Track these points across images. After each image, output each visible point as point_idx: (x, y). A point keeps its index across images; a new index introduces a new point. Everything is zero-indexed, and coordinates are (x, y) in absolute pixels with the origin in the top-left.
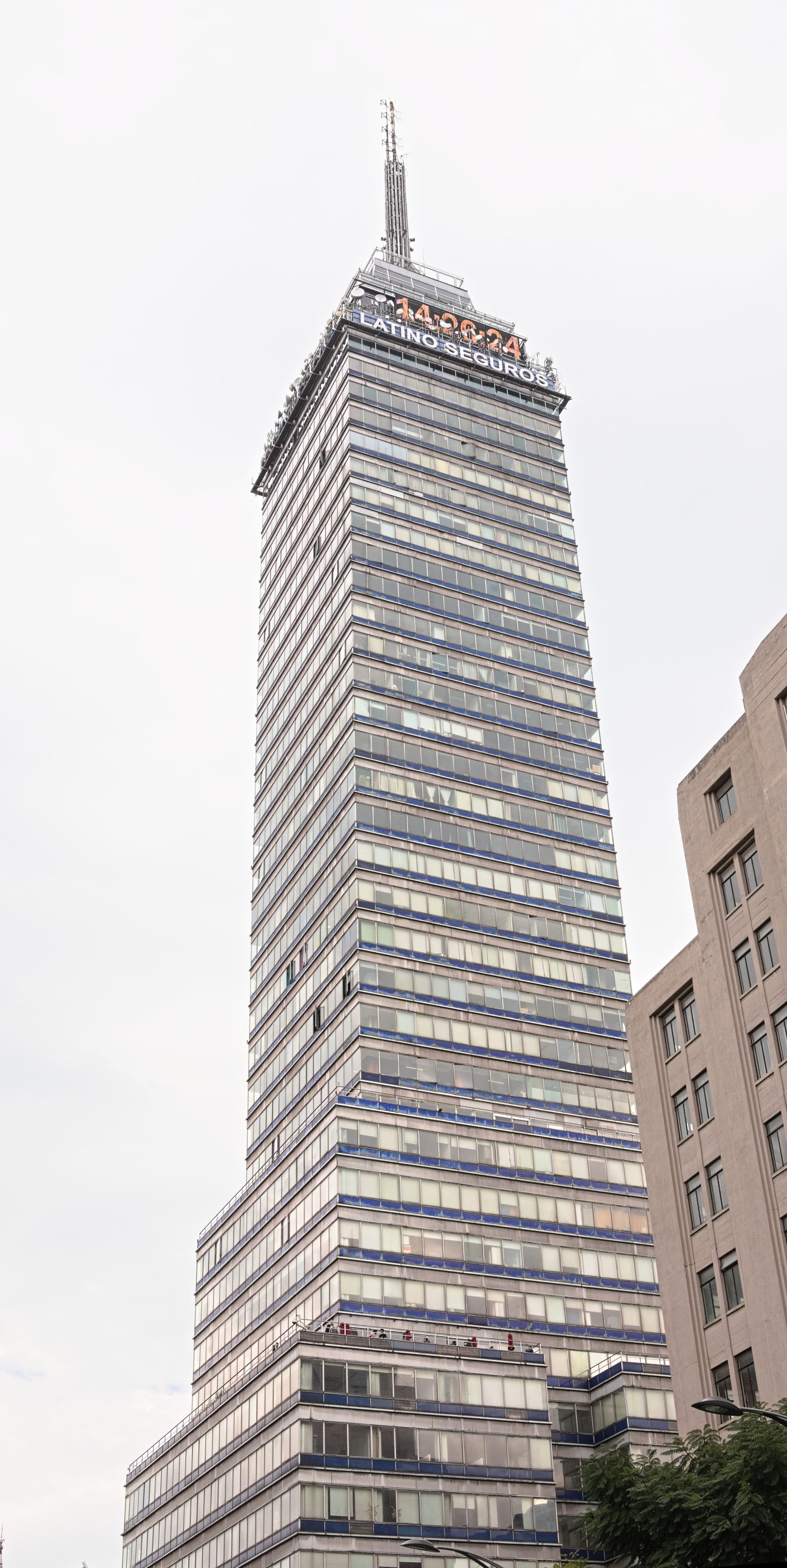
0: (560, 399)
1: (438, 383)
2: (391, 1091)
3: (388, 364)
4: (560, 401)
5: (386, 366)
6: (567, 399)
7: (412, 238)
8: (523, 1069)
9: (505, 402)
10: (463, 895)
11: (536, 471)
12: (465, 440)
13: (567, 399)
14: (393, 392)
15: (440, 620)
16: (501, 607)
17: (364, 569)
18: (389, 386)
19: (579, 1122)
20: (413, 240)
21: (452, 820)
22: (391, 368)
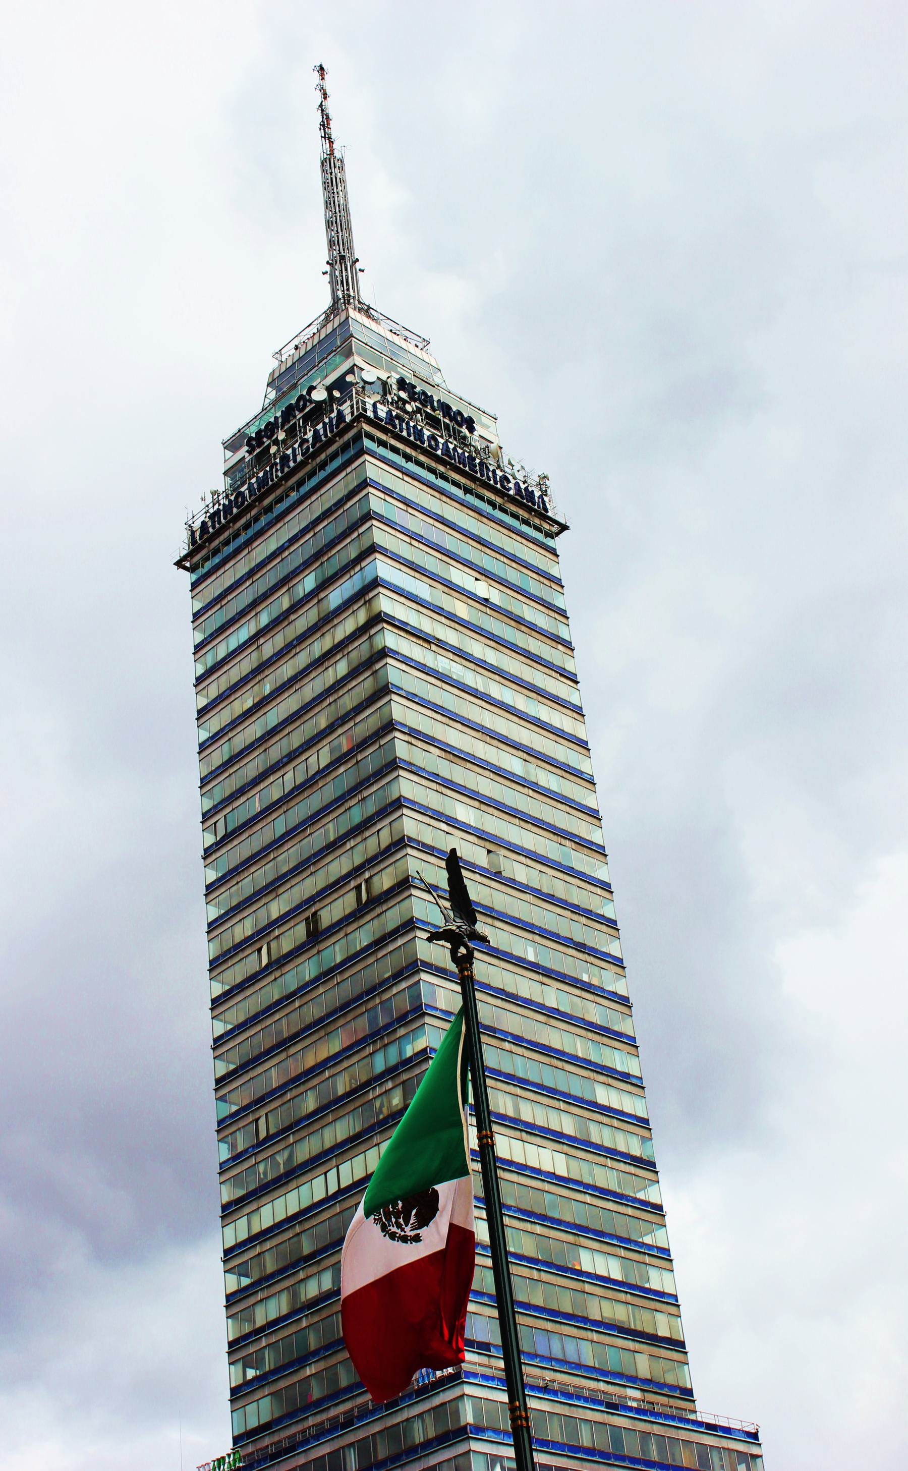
0: (556, 526)
1: (448, 500)
2: (484, 1360)
3: (403, 473)
4: (555, 528)
5: (399, 474)
6: (564, 528)
7: (362, 268)
8: (589, 1335)
9: (510, 529)
10: (524, 1134)
11: (540, 618)
12: (478, 576)
13: (564, 528)
14: (410, 510)
15: (476, 804)
16: (526, 789)
17: (406, 738)
18: (407, 502)
19: (637, 1394)
20: (363, 271)
21: (507, 1046)
22: (406, 478)
